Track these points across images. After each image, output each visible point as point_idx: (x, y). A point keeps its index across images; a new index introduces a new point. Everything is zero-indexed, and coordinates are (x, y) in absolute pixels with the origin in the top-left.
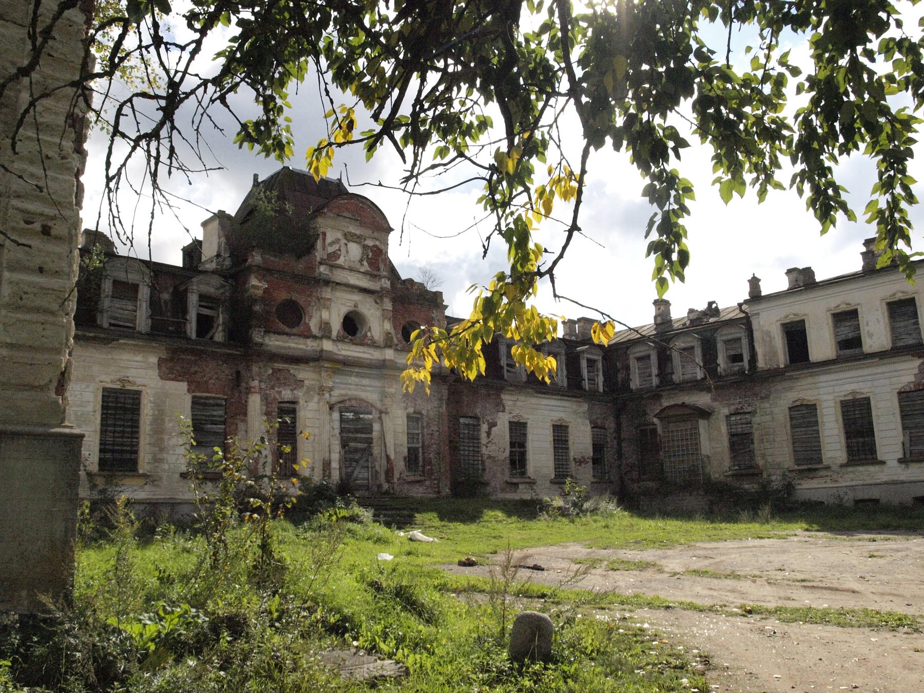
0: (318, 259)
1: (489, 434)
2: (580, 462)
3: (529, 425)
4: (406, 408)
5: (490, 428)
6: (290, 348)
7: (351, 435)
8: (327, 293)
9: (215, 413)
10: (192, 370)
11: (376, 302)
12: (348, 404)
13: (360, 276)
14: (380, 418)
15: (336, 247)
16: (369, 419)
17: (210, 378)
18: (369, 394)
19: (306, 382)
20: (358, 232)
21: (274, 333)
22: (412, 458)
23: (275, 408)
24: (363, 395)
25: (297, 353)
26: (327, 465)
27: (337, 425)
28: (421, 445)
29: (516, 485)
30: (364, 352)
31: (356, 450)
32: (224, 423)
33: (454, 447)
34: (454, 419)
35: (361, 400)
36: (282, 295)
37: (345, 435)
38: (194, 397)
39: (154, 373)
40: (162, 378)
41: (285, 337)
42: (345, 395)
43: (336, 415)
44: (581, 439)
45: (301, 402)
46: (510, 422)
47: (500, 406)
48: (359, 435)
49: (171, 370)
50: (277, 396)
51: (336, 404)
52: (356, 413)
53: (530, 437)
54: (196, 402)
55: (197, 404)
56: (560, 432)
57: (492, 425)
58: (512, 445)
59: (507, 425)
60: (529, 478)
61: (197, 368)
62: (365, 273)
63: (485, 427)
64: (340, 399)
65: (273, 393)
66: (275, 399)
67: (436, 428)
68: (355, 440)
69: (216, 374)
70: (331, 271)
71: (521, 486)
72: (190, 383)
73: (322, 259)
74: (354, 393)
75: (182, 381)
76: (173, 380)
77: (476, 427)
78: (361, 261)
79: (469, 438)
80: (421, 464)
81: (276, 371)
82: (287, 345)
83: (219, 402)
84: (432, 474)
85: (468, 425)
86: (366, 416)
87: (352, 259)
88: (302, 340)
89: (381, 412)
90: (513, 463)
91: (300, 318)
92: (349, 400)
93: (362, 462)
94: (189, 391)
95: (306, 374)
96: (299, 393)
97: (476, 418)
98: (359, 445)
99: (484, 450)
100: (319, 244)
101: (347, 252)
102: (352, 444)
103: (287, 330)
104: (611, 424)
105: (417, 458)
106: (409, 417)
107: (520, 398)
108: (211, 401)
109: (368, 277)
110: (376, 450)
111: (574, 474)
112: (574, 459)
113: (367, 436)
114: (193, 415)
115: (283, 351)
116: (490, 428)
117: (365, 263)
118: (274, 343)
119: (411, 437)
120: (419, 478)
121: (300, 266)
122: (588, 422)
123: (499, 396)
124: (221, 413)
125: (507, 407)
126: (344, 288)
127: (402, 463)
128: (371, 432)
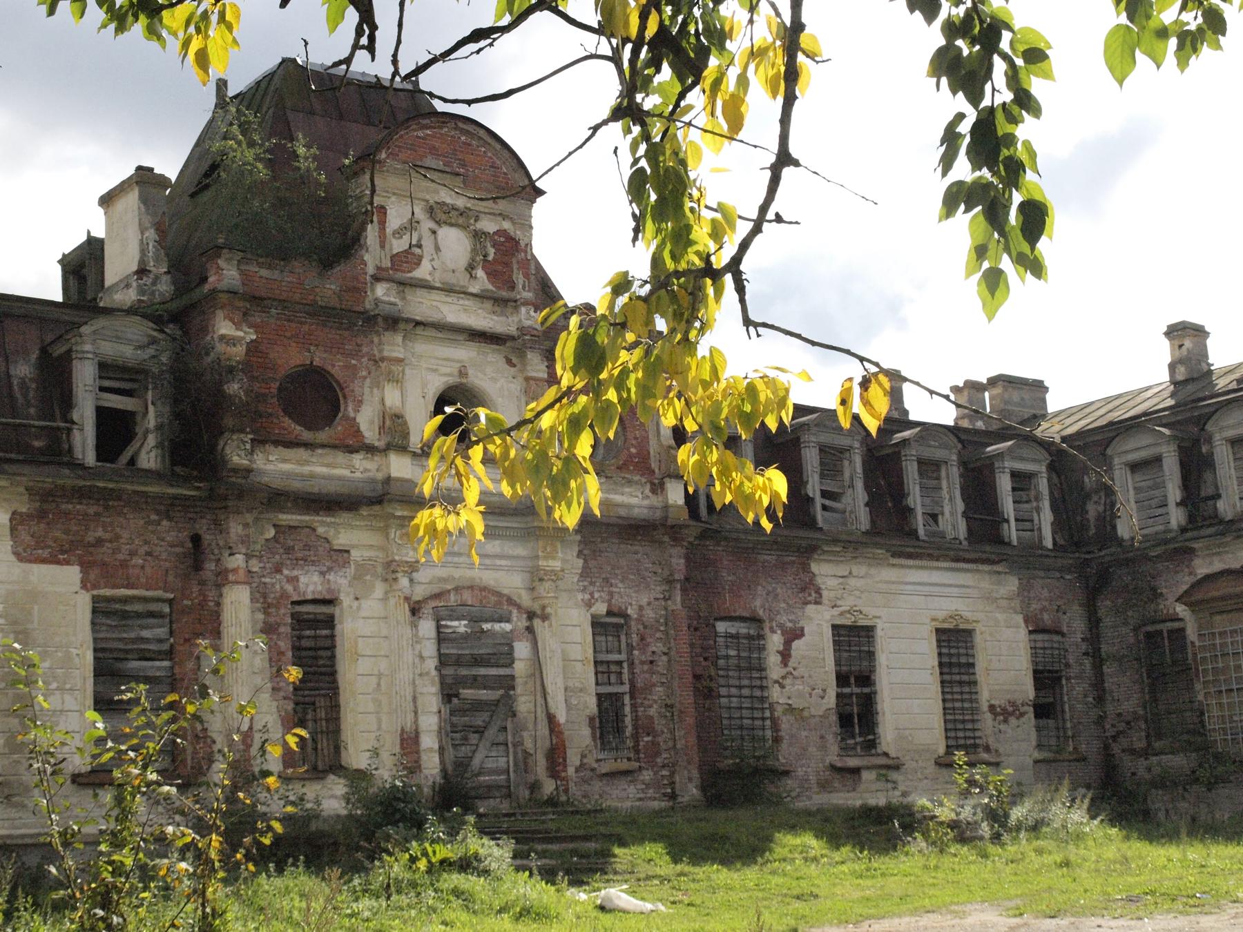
0: (371, 270)
1: (785, 655)
2: (1005, 713)
3: (879, 632)
4: (589, 605)
5: (788, 643)
6: (312, 476)
7: (464, 672)
8: (393, 346)
9: (146, 634)
10: (90, 537)
11: (509, 362)
12: (453, 599)
13: (468, 303)
14: (530, 630)
16: (505, 634)
17: (132, 554)
18: (500, 575)
19: (355, 554)
20: (461, 202)
21: (277, 443)
22: (608, 721)
23: (284, 615)
25: (331, 488)
26: (410, 741)
27: (430, 649)
28: (626, 688)
29: (856, 771)
31: (478, 706)
32: (170, 654)
33: (705, 690)
34: (701, 625)
35: (484, 589)
36: (290, 357)
37: (449, 671)
38: (96, 600)
40: (20, 558)
41: (302, 453)
42: (445, 580)
43: (427, 627)
44: (1006, 662)
45: (346, 600)
46: (834, 627)
47: (809, 591)
48: (483, 671)
49: (40, 543)
50: (289, 588)
51: (426, 600)
52: (475, 620)
53: (882, 659)
54: (101, 610)
55: (107, 614)
56: (954, 645)
57: (794, 634)
58: (842, 679)
59: (828, 633)
60: (886, 754)
61: (100, 533)
62: (481, 296)
63: (775, 641)
64: (435, 589)
65: (277, 583)
66: (284, 595)
67: (659, 647)
68: (475, 682)
69: (144, 543)
70: (401, 294)
71: (865, 775)
72: (85, 566)
73: (379, 268)
75: (67, 563)
76: (44, 561)
77: (756, 642)
78: (470, 268)
79: (739, 668)
80: (629, 731)
82: (306, 469)
83: (153, 607)
84: (658, 754)
85: (736, 636)
86: (497, 627)
87: (451, 266)
88: (341, 457)
89: (531, 615)
90: (845, 720)
91: (336, 408)
92: (456, 589)
93: (491, 733)
94: (84, 586)
95: (353, 535)
96: (341, 581)
97: (755, 620)
98: (484, 694)
99: (775, 694)
100: (371, 232)
102: (467, 693)
103: (307, 435)
104: (1075, 623)
105: (619, 717)
106: (597, 625)
107: (855, 570)
108: (138, 607)
109: (488, 305)
110: (524, 704)
111: (991, 741)
112: (992, 708)
113: (502, 671)
114: (95, 640)
115: (297, 485)
116: (788, 643)
117: (480, 273)
118: (277, 466)
119: (603, 669)
120: (624, 765)
121: (329, 288)
122: (1019, 619)
123: (805, 568)
124: (161, 632)
125: (825, 593)
126: (431, 332)
127: (586, 732)
128: (510, 661)
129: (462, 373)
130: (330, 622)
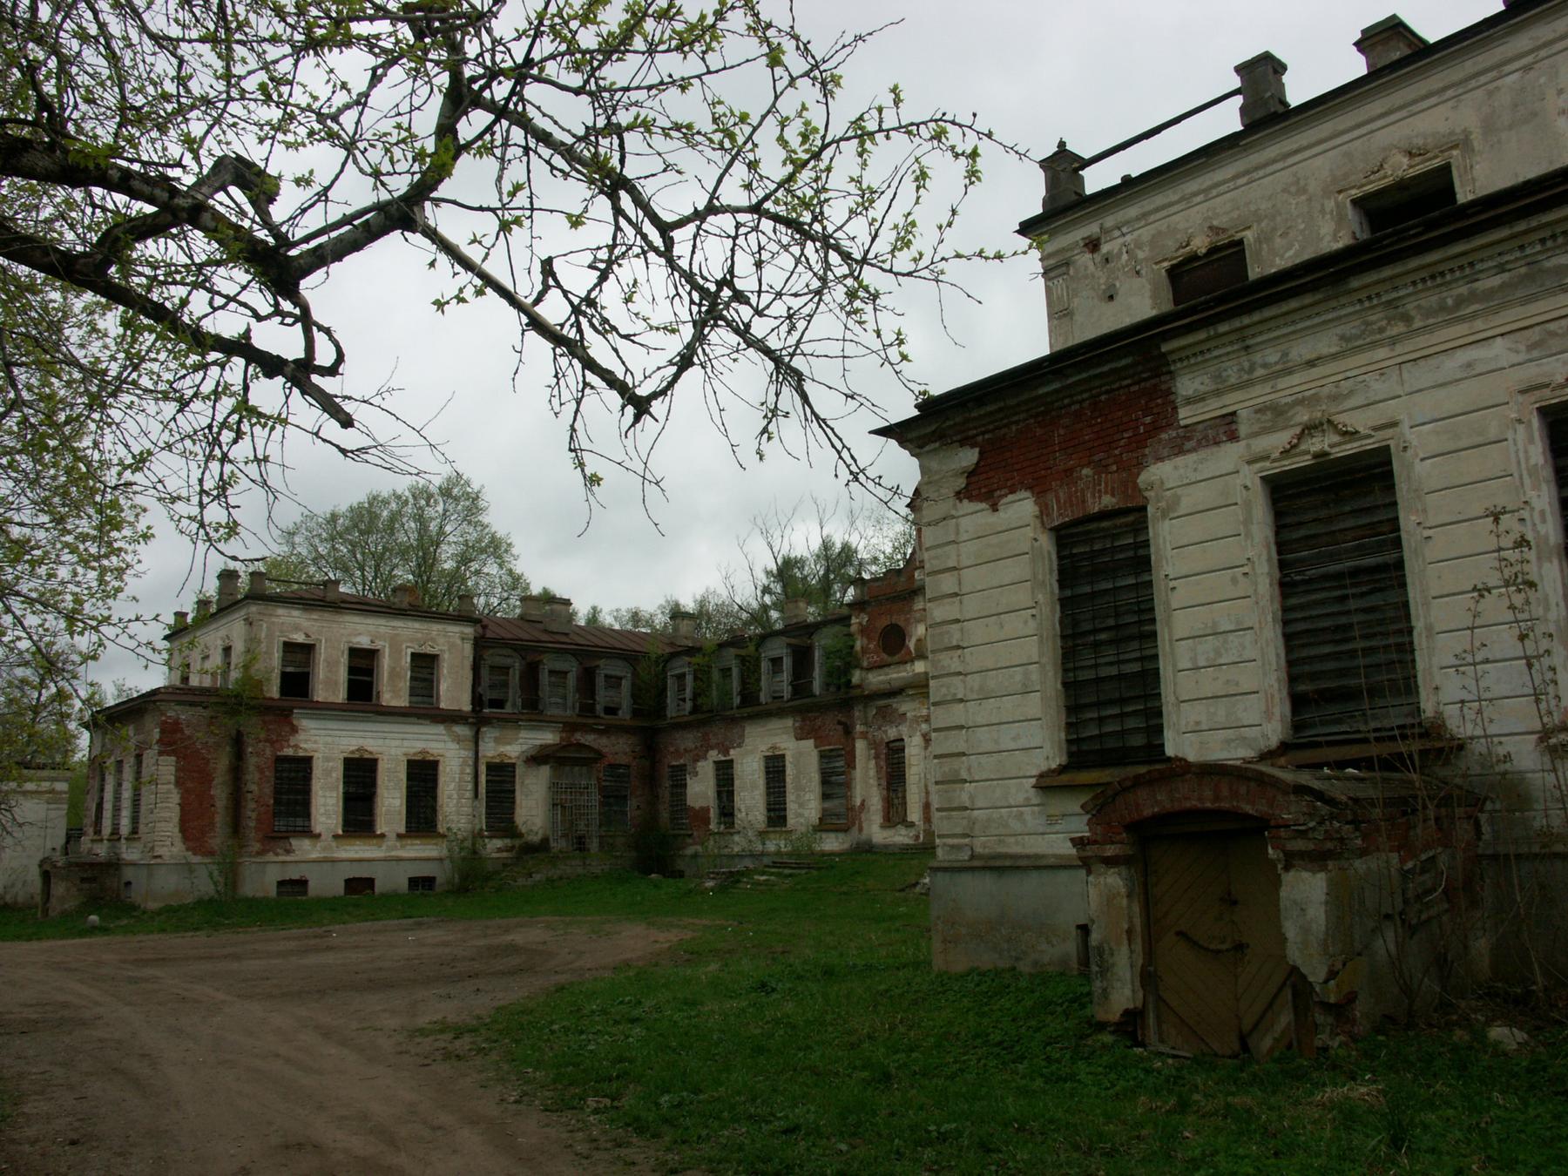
36: (883, 622)
54: (823, 756)
81: (879, 709)
95: (908, 707)
96: (904, 730)
118: (876, 680)
130: (903, 750)
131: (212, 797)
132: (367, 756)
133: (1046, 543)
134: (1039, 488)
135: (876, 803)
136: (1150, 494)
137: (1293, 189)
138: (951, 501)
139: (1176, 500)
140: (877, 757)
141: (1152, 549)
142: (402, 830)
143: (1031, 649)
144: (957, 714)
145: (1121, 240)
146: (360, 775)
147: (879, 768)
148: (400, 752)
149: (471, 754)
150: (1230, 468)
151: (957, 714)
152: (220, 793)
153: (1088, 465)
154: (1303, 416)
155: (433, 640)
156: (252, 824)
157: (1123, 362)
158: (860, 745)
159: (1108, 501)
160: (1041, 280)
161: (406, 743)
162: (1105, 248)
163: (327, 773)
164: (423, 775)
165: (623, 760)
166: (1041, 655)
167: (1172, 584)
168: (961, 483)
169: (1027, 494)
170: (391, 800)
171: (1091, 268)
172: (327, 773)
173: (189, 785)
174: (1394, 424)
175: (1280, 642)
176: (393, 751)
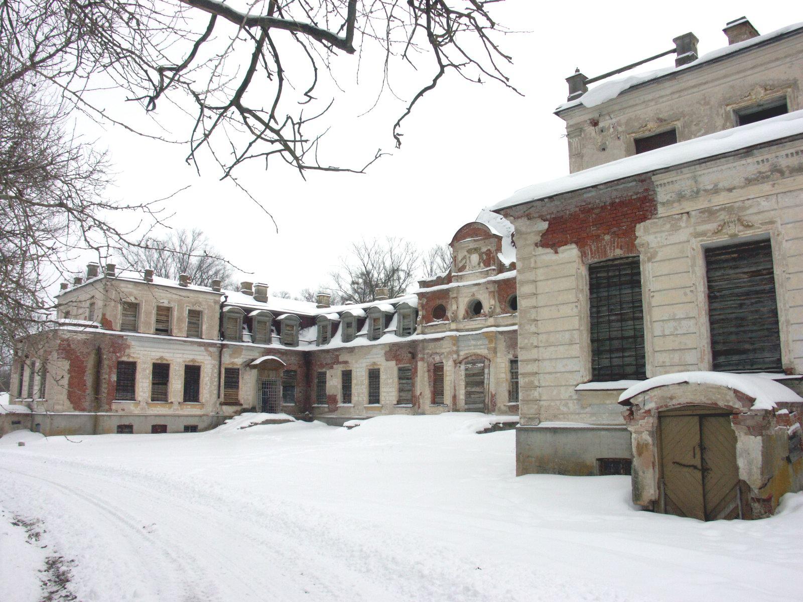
15: (464, 261)
18: (481, 350)
20: (475, 246)
23: (432, 367)
24: (479, 351)
27: (463, 373)
30: (479, 324)
39: (383, 359)
42: (467, 354)
43: (463, 367)
51: (463, 360)
54: (400, 369)
64: (465, 357)
65: (431, 360)
72: (397, 360)
74: (474, 351)
78: (479, 264)
101: (470, 262)
117: (482, 265)
129: (473, 295)
130: (443, 368)
131: (85, 381)
132: (165, 362)
133: (584, 271)
134: (580, 243)
135: (428, 394)
136: (641, 249)
137: (702, 102)
138: (532, 247)
139: (655, 254)
140: (429, 371)
141: (642, 277)
142: (181, 399)
143: (575, 323)
144: (534, 354)
145: (610, 121)
146: (161, 372)
147: (430, 377)
148: (181, 360)
149: (217, 363)
150: (685, 239)
151: (534, 354)
152: (89, 379)
153: (608, 234)
154: (723, 216)
155: (200, 303)
156: (105, 395)
157: (631, 184)
158: (420, 364)
159: (618, 252)
160: (566, 140)
161: (185, 356)
162: (601, 125)
163: (144, 370)
164: (192, 373)
165: (294, 368)
166: (580, 325)
167: (652, 294)
168: (539, 238)
169: (574, 246)
170: (176, 384)
171: (593, 134)
172: (144, 370)
173: (73, 374)
174: (772, 222)
175: (708, 324)
176: (178, 360)
